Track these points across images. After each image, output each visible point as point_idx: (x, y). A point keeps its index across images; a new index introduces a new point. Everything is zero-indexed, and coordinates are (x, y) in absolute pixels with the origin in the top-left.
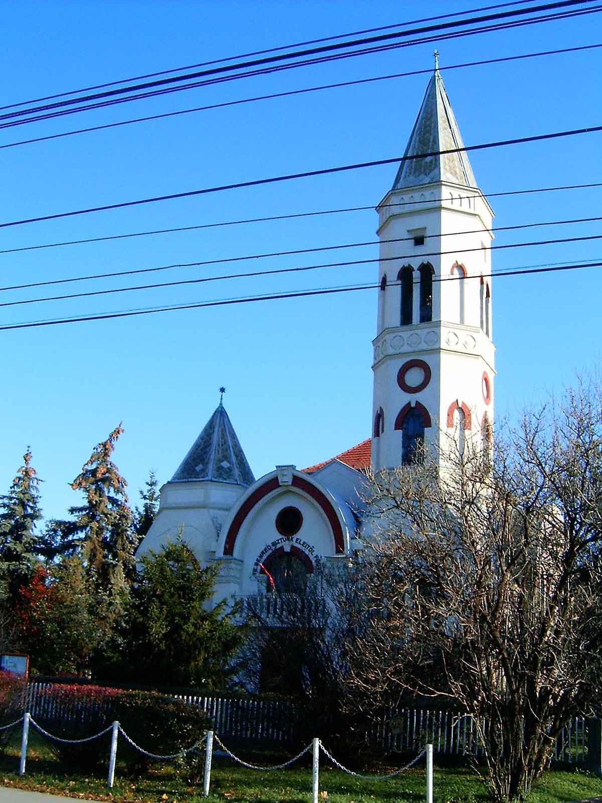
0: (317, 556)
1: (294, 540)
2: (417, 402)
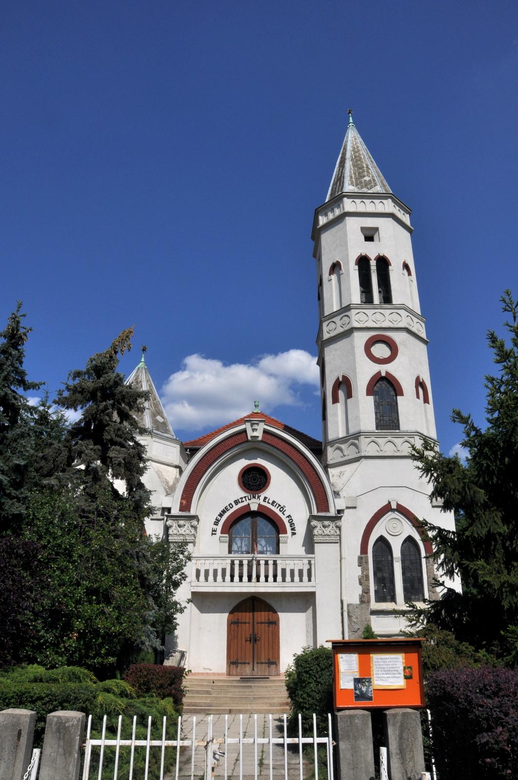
1: (262, 498)
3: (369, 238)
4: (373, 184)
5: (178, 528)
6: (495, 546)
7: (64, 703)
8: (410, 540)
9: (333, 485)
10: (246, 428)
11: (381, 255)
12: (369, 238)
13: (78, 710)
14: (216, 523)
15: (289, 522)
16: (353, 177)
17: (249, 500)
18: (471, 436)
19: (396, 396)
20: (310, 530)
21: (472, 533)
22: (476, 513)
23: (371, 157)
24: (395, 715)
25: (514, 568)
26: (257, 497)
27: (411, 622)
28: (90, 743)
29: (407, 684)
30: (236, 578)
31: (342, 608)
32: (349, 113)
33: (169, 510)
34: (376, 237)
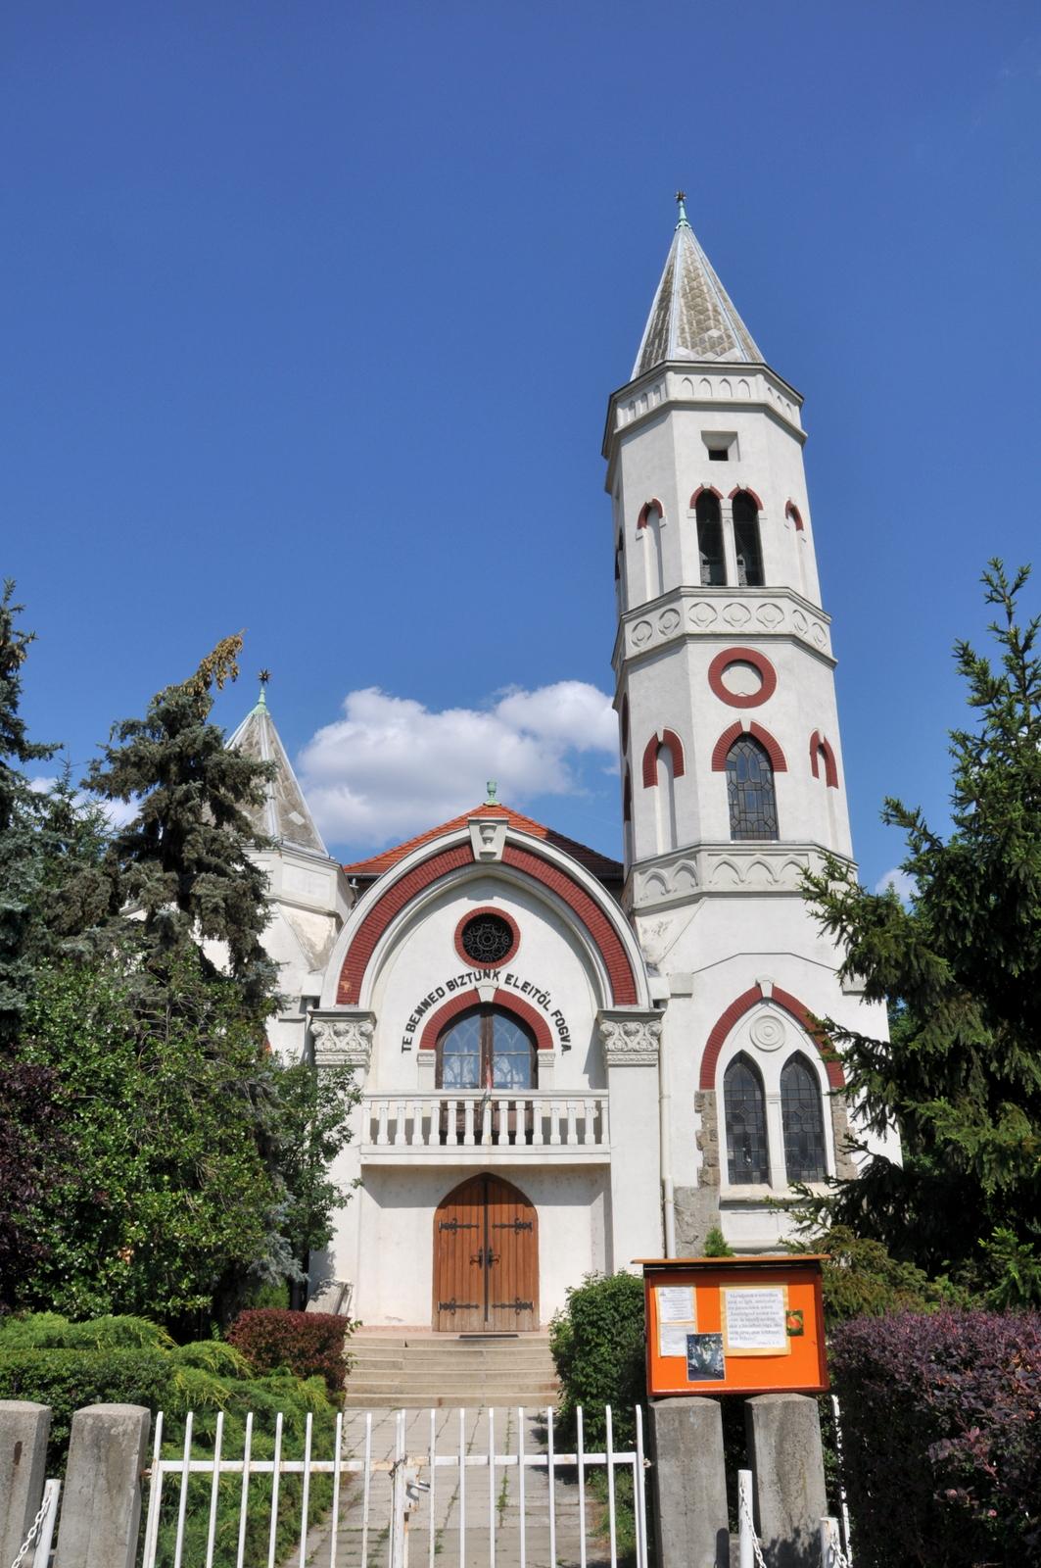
0: (557, 1013)
1: (502, 977)
2: (754, 725)
3: (718, 455)
4: (726, 345)
5: (335, 1038)
6: (968, 1071)
7: (108, 1388)
8: (798, 1059)
9: (644, 950)
10: (470, 836)
11: (743, 487)
12: (718, 455)
13: (136, 1403)
14: (411, 1028)
15: (558, 1025)
16: (687, 330)
17: (477, 980)
18: (922, 851)
19: (772, 771)
20: (599, 1040)
21: (924, 1045)
22: (930, 1004)
23: (723, 288)
24: (768, 1408)
25: (1007, 1115)
26: (492, 975)
27: (801, 1222)
28: (160, 1469)
29: (793, 1346)
30: (452, 1137)
31: (663, 1197)
32: (680, 199)
33: (316, 1001)
34: (731, 452)
